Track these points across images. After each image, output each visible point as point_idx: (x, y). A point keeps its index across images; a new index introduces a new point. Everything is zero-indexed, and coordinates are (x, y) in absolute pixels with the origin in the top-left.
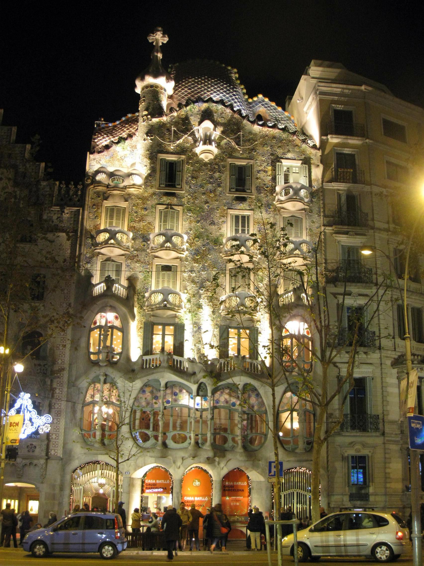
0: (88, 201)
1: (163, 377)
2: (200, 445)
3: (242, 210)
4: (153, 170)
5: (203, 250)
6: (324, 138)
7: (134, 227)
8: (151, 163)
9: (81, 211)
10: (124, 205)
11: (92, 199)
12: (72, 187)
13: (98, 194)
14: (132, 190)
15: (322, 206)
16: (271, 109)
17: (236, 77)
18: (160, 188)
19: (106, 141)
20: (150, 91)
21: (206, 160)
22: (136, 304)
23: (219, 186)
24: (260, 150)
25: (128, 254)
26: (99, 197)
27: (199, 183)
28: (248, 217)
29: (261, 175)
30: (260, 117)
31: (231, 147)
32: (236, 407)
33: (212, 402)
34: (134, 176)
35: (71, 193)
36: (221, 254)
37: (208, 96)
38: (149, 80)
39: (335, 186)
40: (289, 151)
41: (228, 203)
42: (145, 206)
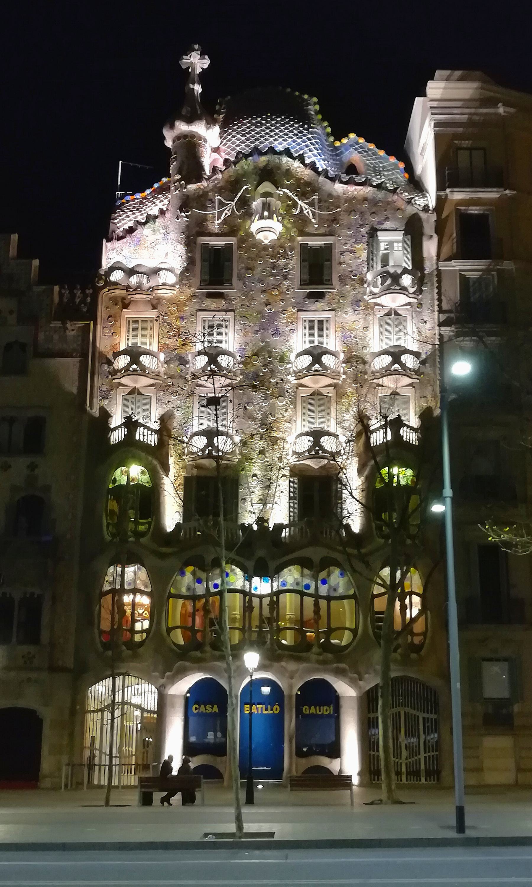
0: (102, 312)
3: (317, 312)
4: (190, 261)
6: (442, 193)
7: (167, 345)
8: (187, 252)
11: (107, 308)
12: (79, 293)
13: (115, 301)
14: (162, 293)
15: (436, 297)
16: (369, 155)
17: (316, 110)
19: (130, 221)
20: (184, 143)
21: (266, 242)
22: (172, 452)
23: (285, 278)
24: (345, 219)
26: (116, 305)
27: (257, 277)
28: (328, 320)
29: (347, 258)
30: (351, 169)
34: (162, 273)
35: (77, 301)
37: (271, 143)
38: (182, 127)
39: (456, 265)
40: (387, 219)
41: (298, 303)
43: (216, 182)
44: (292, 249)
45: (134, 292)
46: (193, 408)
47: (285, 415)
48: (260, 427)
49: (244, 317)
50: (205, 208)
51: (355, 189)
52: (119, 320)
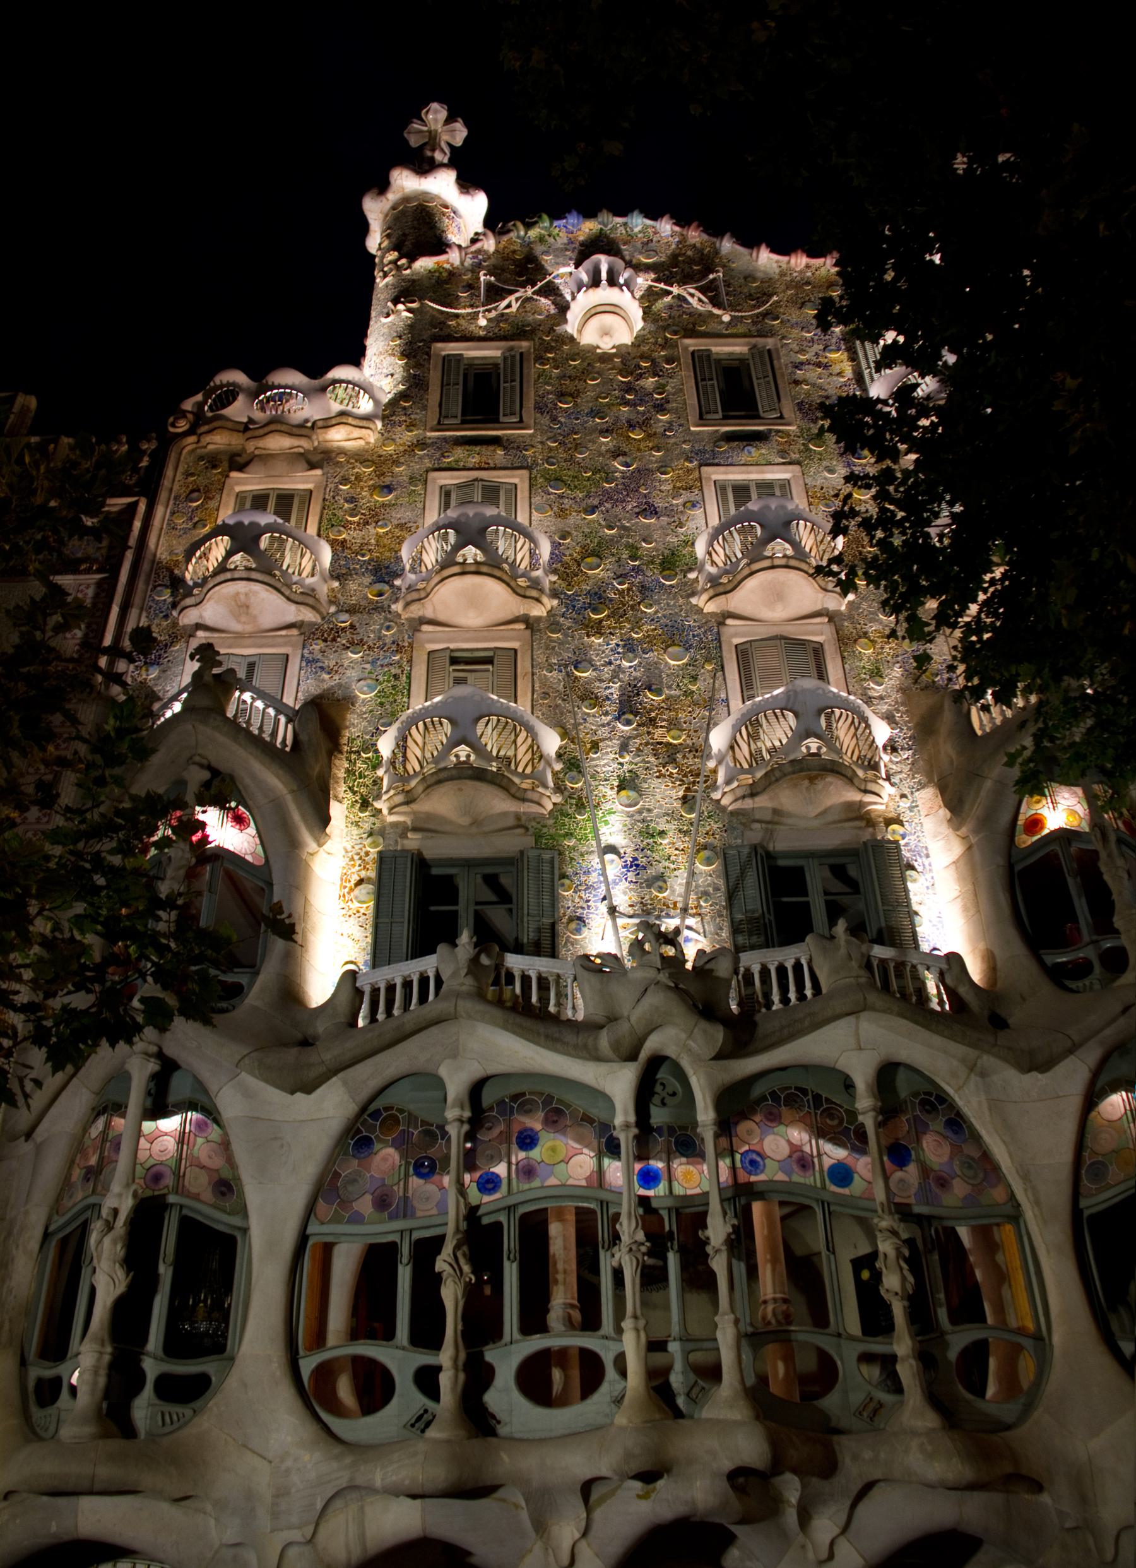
0: (173, 479)
1: (454, 1054)
2: (681, 1401)
5: (621, 593)
8: (406, 368)
9: (142, 507)
10: (303, 481)
11: (192, 475)
13: (213, 461)
14: (338, 437)
18: (440, 426)
21: (606, 345)
22: (341, 789)
23: (660, 408)
25: (315, 624)
26: (215, 467)
29: (812, 374)
31: (690, 314)
32: (857, 1186)
33: (724, 1165)
36: (694, 601)
38: (405, 182)
42: (387, 480)
43: (480, 257)
44: (669, 361)
45: (262, 432)
46: (409, 677)
47: (694, 688)
48: (618, 718)
49: (556, 479)
50: (450, 300)
51: (808, 266)
52: (218, 496)
